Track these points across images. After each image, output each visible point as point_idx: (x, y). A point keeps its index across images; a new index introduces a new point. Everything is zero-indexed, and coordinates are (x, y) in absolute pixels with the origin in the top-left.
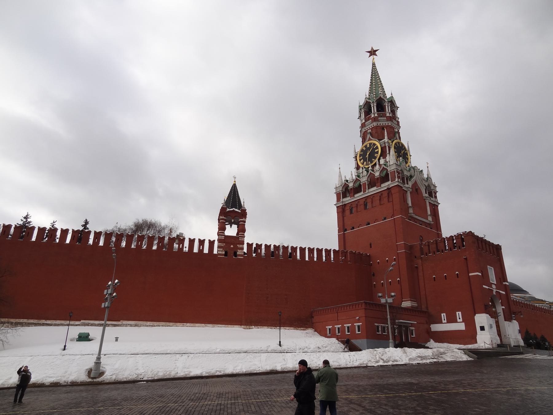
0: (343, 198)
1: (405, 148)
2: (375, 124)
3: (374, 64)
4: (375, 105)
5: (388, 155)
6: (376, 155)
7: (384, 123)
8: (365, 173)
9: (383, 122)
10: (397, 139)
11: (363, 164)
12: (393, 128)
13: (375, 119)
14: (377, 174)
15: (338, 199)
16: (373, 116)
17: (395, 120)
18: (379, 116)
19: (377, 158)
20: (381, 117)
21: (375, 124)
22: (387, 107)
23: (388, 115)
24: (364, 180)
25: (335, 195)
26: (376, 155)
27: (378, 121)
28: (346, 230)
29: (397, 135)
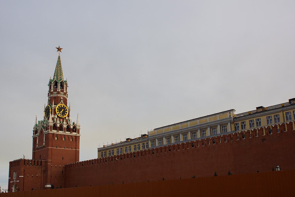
1: (65, 108)
3: (59, 57)
4: (53, 85)
9: (55, 95)
10: (62, 103)
11: (46, 116)
12: (60, 97)
13: (52, 93)
17: (63, 92)
18: (54, 91)
20: (55, 92)
22: (58, 86)
23: (58, 90)
27: (53, 94)
28: (35, 150)
29: (62, 101)
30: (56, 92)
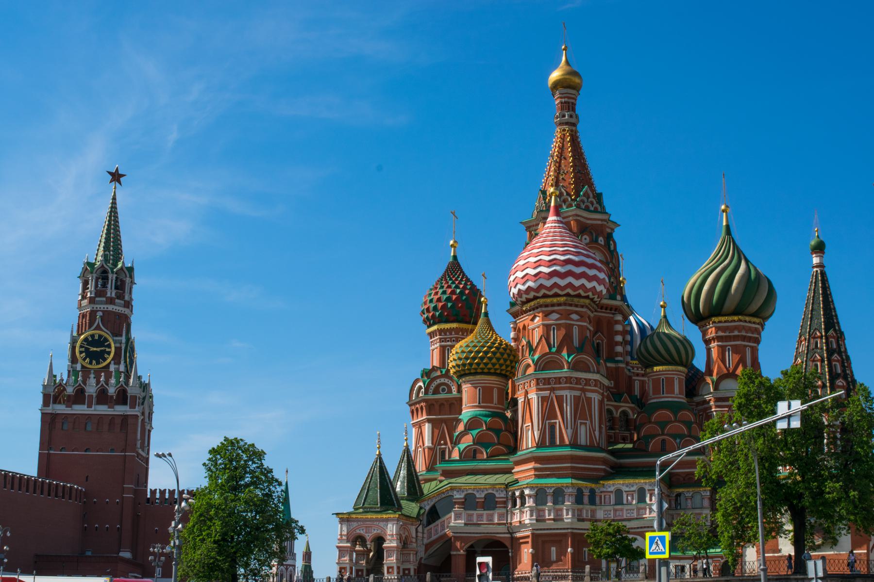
0: (55, 402)
2: (111, 307)
5: (122, 362)
6: (106, 356)
7: (121, 309)
8: (92, 381)
13: (111, 301)
14: (112, 391)
15: (46, 403)
16: (109, 295)
19: (108, 361)
21: (111, 307)
23: (127, 298)
24: (91, 388)
25: (42, 395)
26: (106, 356)
27: (114, 304)
28: (51, 449)
30: (123, 302)
